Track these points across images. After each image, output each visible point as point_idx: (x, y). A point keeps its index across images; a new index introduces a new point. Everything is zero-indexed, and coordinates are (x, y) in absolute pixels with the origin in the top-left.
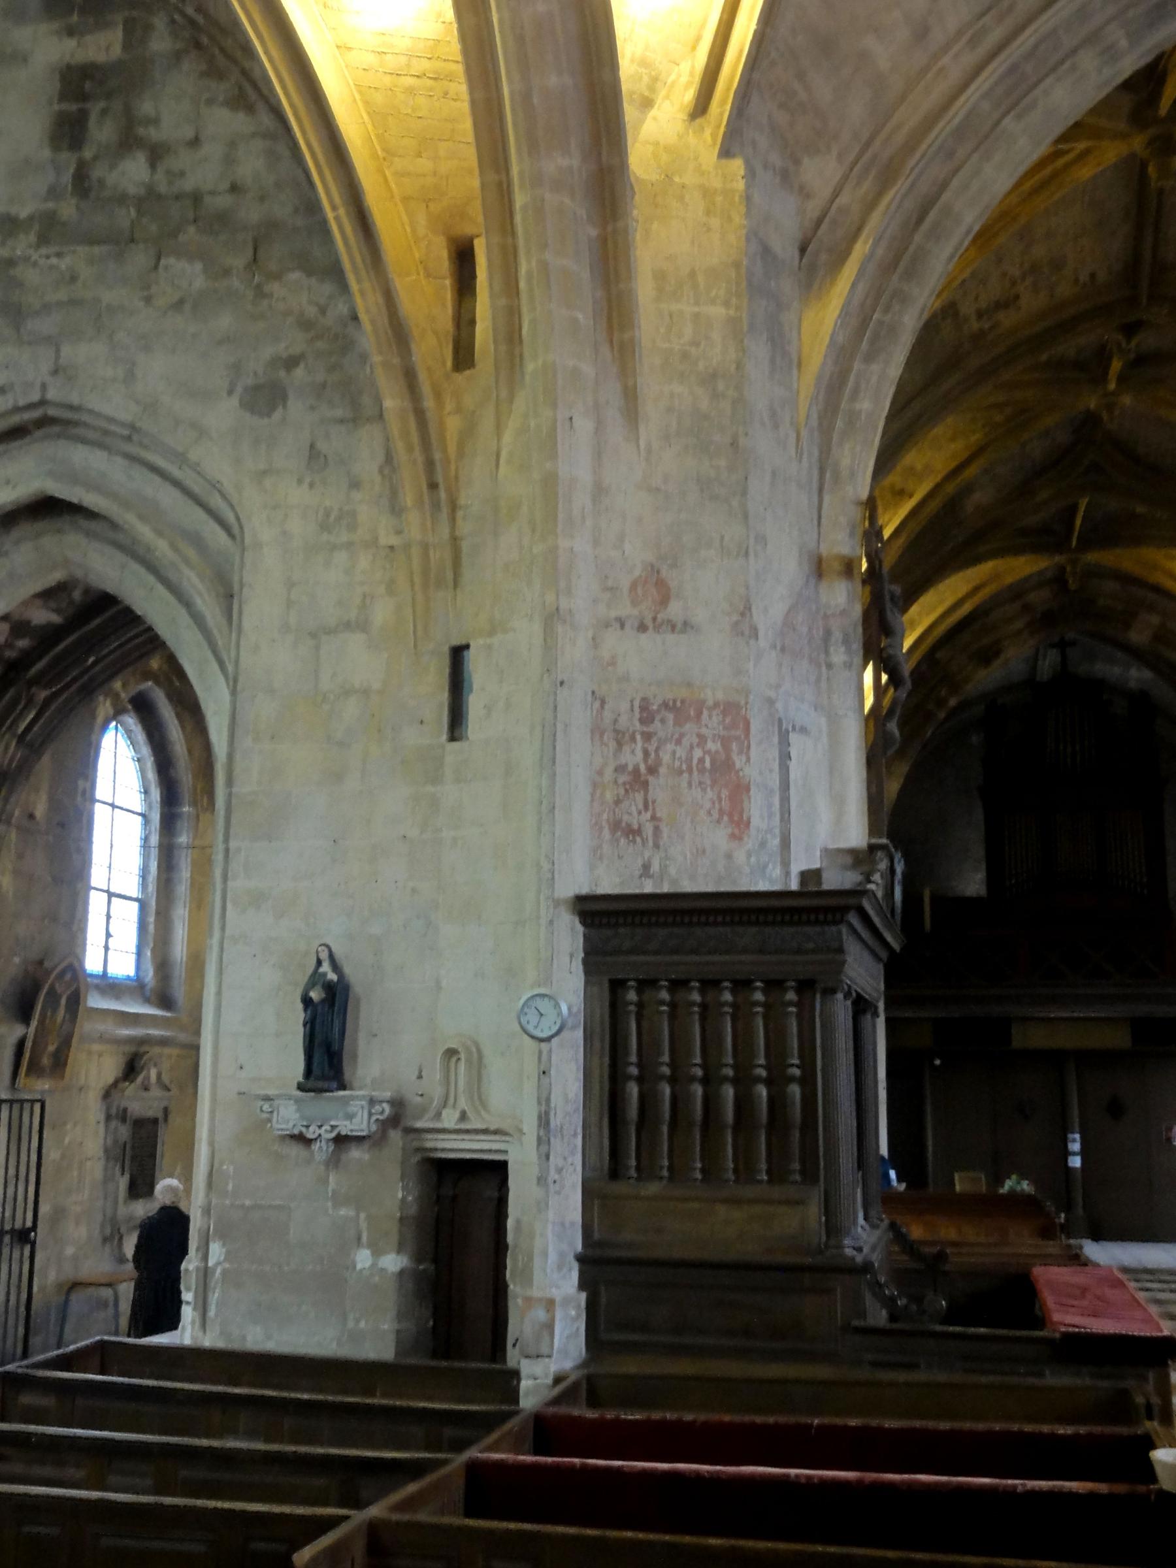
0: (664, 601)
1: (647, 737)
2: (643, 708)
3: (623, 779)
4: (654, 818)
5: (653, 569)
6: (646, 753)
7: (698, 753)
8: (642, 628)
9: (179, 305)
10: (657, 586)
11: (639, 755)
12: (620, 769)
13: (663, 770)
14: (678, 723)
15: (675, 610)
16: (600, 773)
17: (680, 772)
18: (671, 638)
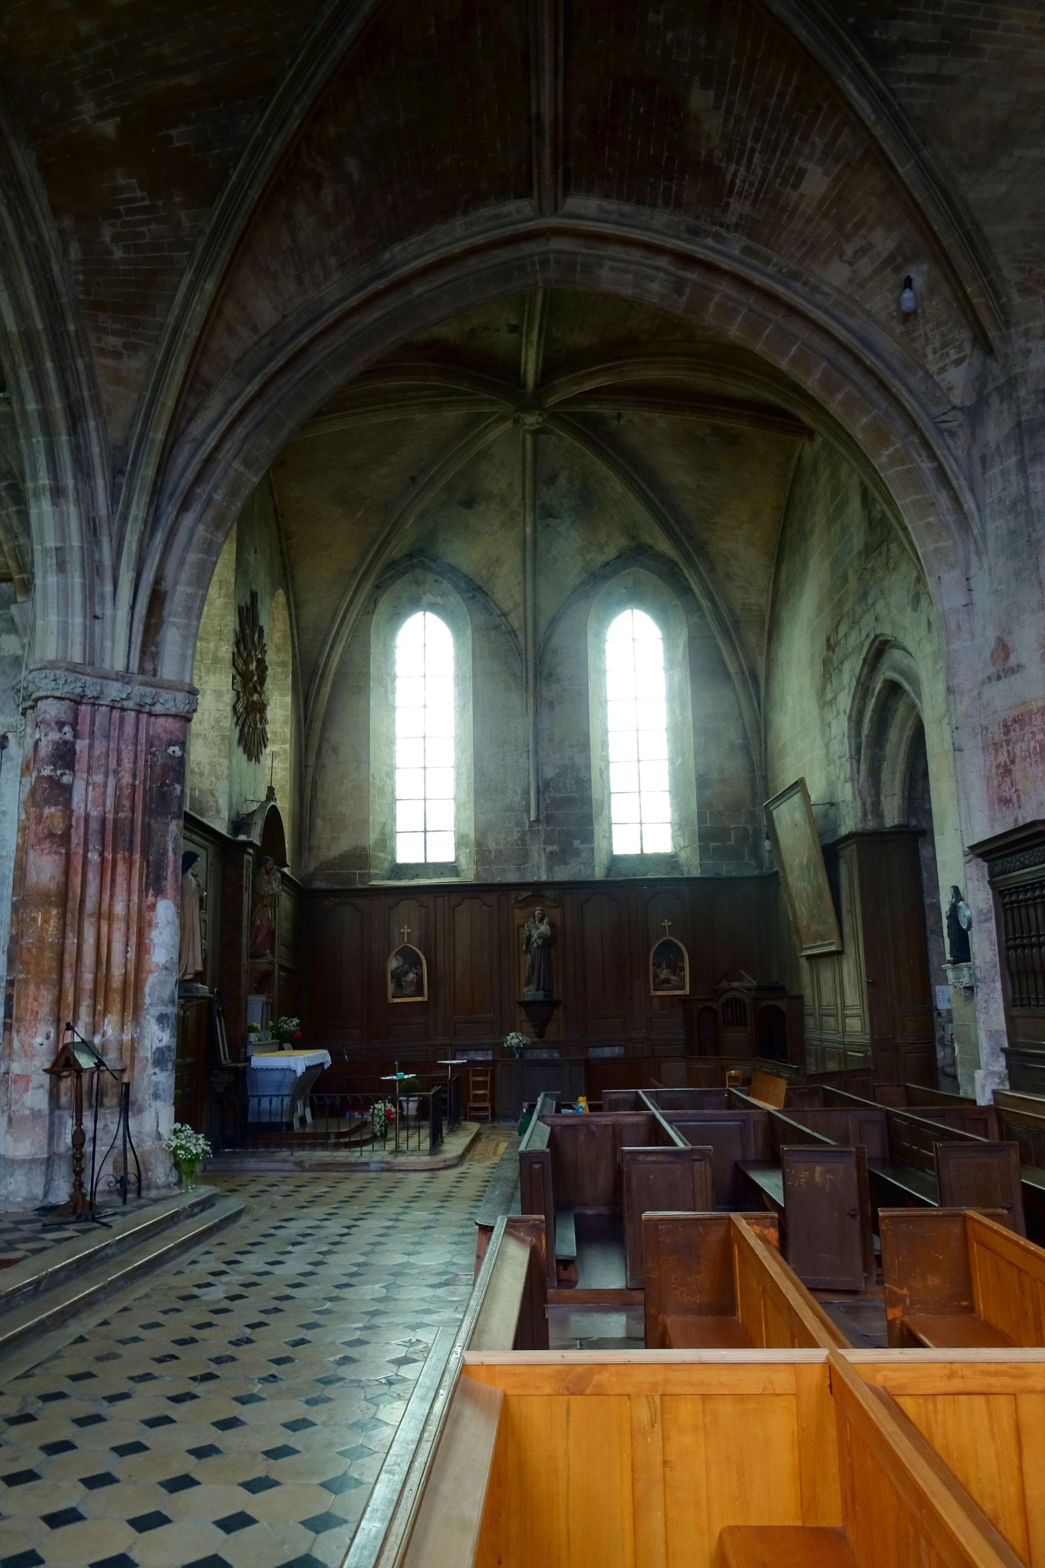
0: (1007, 657)
1: (1008, 742)
2: (1005, 726)
3: (1001, 770)
4: (1017, 790)
5: (1000, 640)
6: (1008, 751)
7: (1033, 744)
8: (999, 678)
9: (894, 569)
10: (1003, 649)
11: (1005, 753)
12: (998, 767)
13: (1017, 760)
14: (1021, 730)
15: (1013, 661)
16: (990, 771)
17: (1025, 758)
18: (1013, 678)
